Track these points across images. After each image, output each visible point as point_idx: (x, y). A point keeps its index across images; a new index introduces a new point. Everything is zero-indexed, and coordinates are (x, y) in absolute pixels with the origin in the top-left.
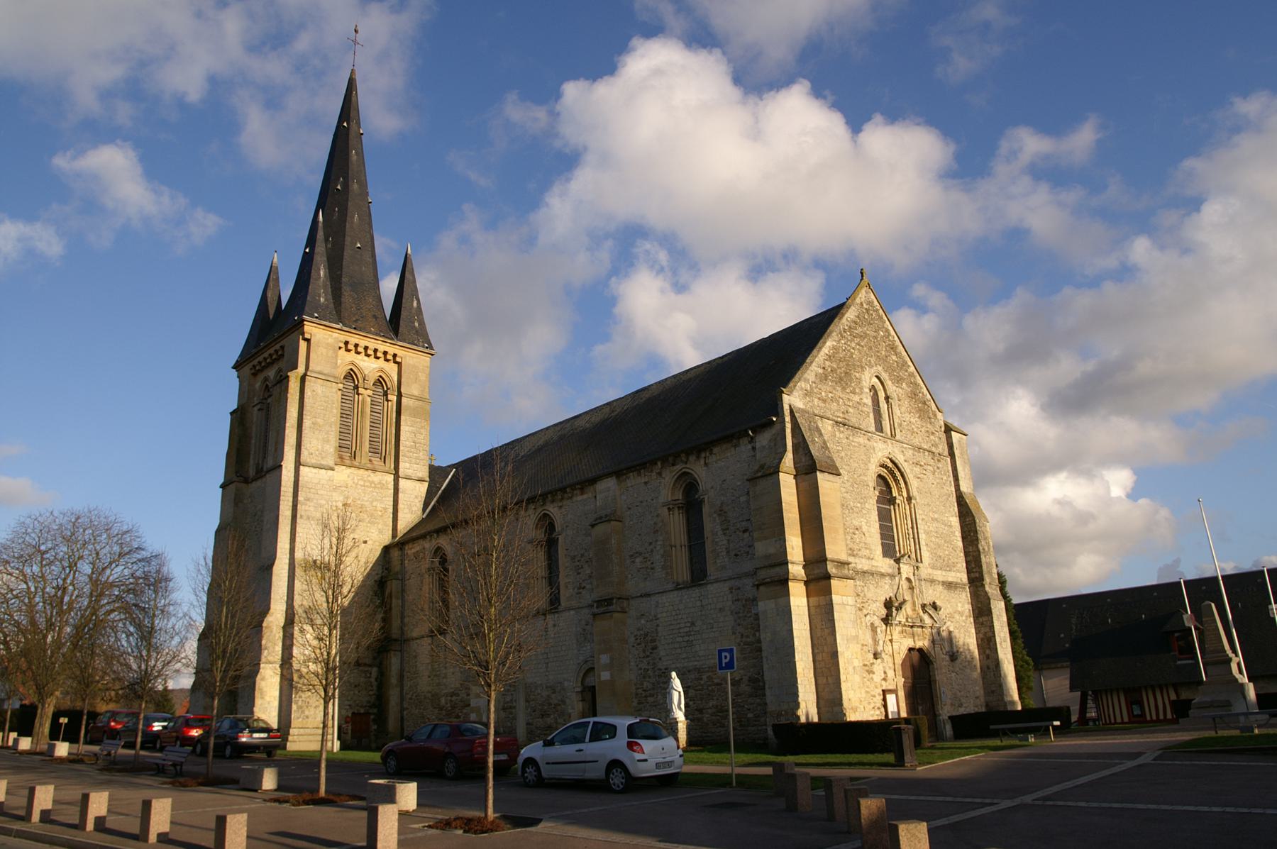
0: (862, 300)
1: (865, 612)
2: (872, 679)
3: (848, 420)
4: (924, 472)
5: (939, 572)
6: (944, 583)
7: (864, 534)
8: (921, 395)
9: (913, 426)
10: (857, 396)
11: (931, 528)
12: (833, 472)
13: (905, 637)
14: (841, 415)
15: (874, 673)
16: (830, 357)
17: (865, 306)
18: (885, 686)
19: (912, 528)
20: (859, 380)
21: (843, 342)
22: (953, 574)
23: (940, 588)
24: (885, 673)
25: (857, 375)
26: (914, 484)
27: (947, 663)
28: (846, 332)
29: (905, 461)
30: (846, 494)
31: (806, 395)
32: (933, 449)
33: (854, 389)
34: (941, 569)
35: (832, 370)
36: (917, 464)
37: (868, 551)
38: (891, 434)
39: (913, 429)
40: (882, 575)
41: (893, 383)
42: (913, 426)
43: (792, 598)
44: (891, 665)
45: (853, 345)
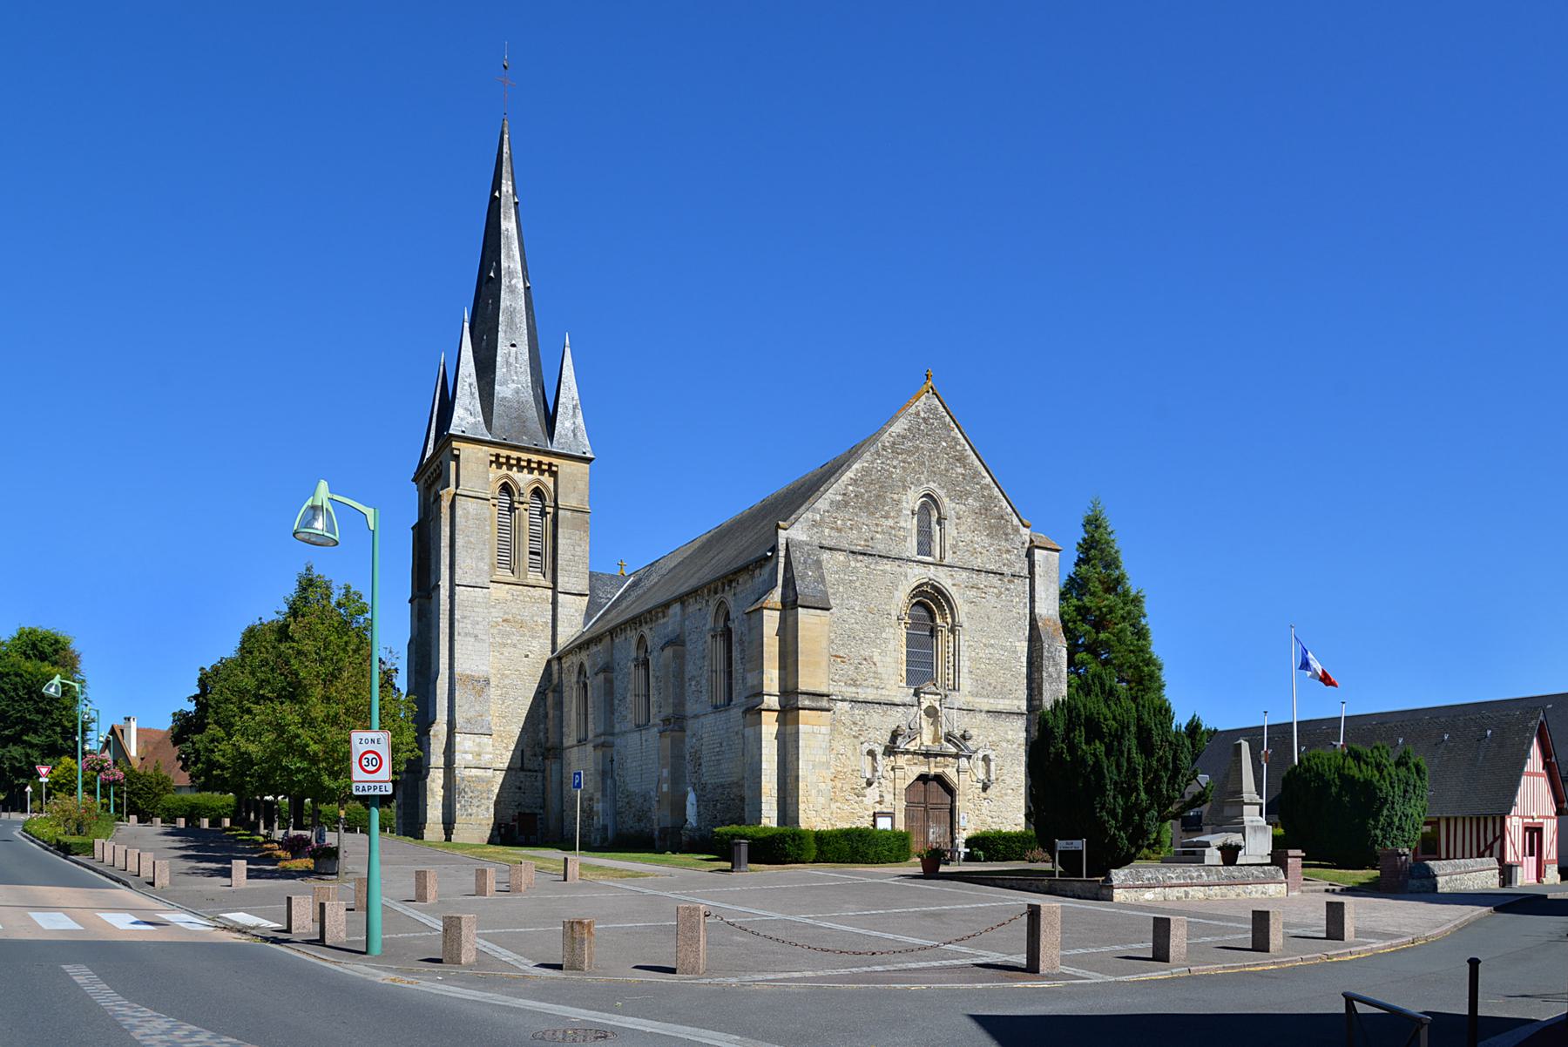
0: (919, 408)
1: (862, 739)
2: (862, 801)
4: (983, 595)
5: (986, 700)
7: (875, 665)
8: (997, 509)
9: (976, 546)
10: (890, 520)
11: (980, 655)
13: (916, 764)
14: (863, 543)
15: (865, 796)
16: (856, 481)
17: (922, 415)
19: (954, 655)
20: (898, 502)
21: (879, 461)
22: (1007, 702)
24: (881, 796)
25: (895, 497)
26: (962, 609)
28: (885, 450)
29: (954, 585)
30: (855, 625)
31: (813, 525)
32: (1005, 570)
33: (887, 512)
35: (856, 496)
36: (972, 587)
37: (877, 681)
38: (941, 558)
39: (975, 549)
41: (950, 500)
42: (976, 546)
43: (764, 727)
44: (892, 790)
45: (895, 463)
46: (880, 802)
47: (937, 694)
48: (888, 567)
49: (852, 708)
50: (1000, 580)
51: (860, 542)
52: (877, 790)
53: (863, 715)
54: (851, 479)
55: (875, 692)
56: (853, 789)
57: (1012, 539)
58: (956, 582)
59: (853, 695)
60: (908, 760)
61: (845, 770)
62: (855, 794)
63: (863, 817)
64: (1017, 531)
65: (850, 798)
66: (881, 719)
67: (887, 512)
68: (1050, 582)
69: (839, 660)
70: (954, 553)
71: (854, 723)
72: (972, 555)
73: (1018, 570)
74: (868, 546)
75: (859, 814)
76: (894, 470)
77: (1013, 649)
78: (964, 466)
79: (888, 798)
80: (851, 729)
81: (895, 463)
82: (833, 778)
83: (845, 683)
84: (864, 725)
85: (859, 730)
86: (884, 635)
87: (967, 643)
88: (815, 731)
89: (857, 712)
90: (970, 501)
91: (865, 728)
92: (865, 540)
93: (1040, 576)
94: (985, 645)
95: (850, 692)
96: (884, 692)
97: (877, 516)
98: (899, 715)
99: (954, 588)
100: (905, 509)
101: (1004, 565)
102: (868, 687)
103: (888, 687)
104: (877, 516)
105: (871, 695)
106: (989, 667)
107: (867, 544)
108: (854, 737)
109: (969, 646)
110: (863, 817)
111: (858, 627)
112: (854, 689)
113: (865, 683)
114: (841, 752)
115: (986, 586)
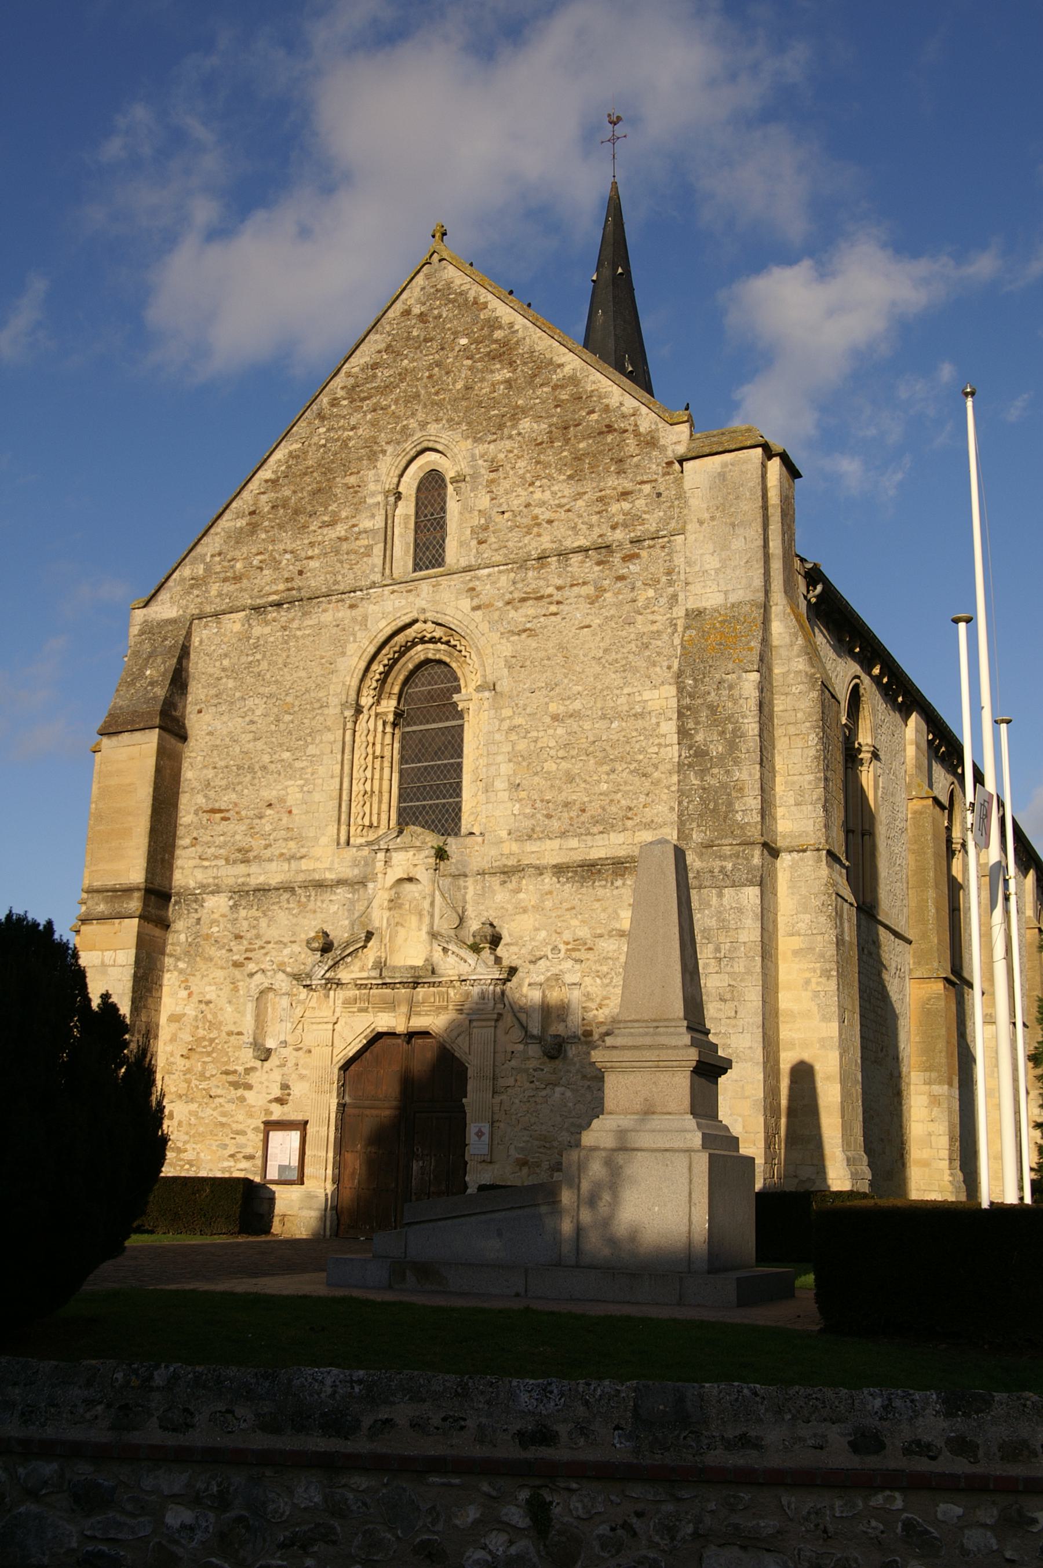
2: (242, 1099)
3: (299, 589)
4: (553, 608)
5: (556, 844)
6: (559, 870)
7: (290, 812)
9: (537, 511)
12: (137, 726)
15: (249, 1087)
18: (277, 1113)
20: (355, 489)
23: (548, 880)
24: (285, 1087)
25: (352, 480)
27: (532, 1064)
33: (334, 514)
34: (563, 834)
36: (523, 600)
37: (292, 844)
39: (536, 518)
40: (320, 885)
42: (537, 511)
46: (281, 1101)
47: (419, 849)
48: (327, 617)
49: (234, 907)
50: (599, 563)
51: (274, 588)
52: (277, 1076)
53: (256, 919)
54: (266, 481)
55: (286, 866)
56: (227, 1073)
57: (637, 466)
58: (484, 599)
59: (240, 880)
60: (347, 1002)
61: (211, 1036)
62: (231, 1084)
63: (243, 1133)
64: (650, 442)
65: (219, 1092)
66: (294, 921)
67: (334, 514)
68: (733, 525)
69: (218, 816)
70: (480, 543)
71: (238, 937)
72: (529, 533)
73: (653, 529)
74: (292, 589)
75: (235, 1126)
76: (351, 433)
77: (638, 709)
78: (511, 363)
79: (298, 1089)
80: (231, 950)
81: (357, 417)
82: (185, 1052)
83: (227, 860)
84: (258, 936)
85: (247, 950)
86: (311, 750)
87: (506, 725)
88: (107, 962)
89: (243, 913)
90: (526, 424)
91: (260, 943)
92: (287, 580)
93: (701, 523)
94: (555, 718)
95: (233, 874)
96: (304, 864)
97: (312, 528)
98: (334, 908)
99: (479, 613)
100: (373, 494)
101: (614, 528)
102: (270, 860)
103: (317, 851)
104: (312, 528)
105: (273, 874)
106: (564, 765)
107: (289, 585)
108: (237, 965)
109: (512, 729)
110: (243, 1133)
111: (260, 744)
112: (242, 869)
113: (268, 853)
114: (208, 997)
115: (559, 588)
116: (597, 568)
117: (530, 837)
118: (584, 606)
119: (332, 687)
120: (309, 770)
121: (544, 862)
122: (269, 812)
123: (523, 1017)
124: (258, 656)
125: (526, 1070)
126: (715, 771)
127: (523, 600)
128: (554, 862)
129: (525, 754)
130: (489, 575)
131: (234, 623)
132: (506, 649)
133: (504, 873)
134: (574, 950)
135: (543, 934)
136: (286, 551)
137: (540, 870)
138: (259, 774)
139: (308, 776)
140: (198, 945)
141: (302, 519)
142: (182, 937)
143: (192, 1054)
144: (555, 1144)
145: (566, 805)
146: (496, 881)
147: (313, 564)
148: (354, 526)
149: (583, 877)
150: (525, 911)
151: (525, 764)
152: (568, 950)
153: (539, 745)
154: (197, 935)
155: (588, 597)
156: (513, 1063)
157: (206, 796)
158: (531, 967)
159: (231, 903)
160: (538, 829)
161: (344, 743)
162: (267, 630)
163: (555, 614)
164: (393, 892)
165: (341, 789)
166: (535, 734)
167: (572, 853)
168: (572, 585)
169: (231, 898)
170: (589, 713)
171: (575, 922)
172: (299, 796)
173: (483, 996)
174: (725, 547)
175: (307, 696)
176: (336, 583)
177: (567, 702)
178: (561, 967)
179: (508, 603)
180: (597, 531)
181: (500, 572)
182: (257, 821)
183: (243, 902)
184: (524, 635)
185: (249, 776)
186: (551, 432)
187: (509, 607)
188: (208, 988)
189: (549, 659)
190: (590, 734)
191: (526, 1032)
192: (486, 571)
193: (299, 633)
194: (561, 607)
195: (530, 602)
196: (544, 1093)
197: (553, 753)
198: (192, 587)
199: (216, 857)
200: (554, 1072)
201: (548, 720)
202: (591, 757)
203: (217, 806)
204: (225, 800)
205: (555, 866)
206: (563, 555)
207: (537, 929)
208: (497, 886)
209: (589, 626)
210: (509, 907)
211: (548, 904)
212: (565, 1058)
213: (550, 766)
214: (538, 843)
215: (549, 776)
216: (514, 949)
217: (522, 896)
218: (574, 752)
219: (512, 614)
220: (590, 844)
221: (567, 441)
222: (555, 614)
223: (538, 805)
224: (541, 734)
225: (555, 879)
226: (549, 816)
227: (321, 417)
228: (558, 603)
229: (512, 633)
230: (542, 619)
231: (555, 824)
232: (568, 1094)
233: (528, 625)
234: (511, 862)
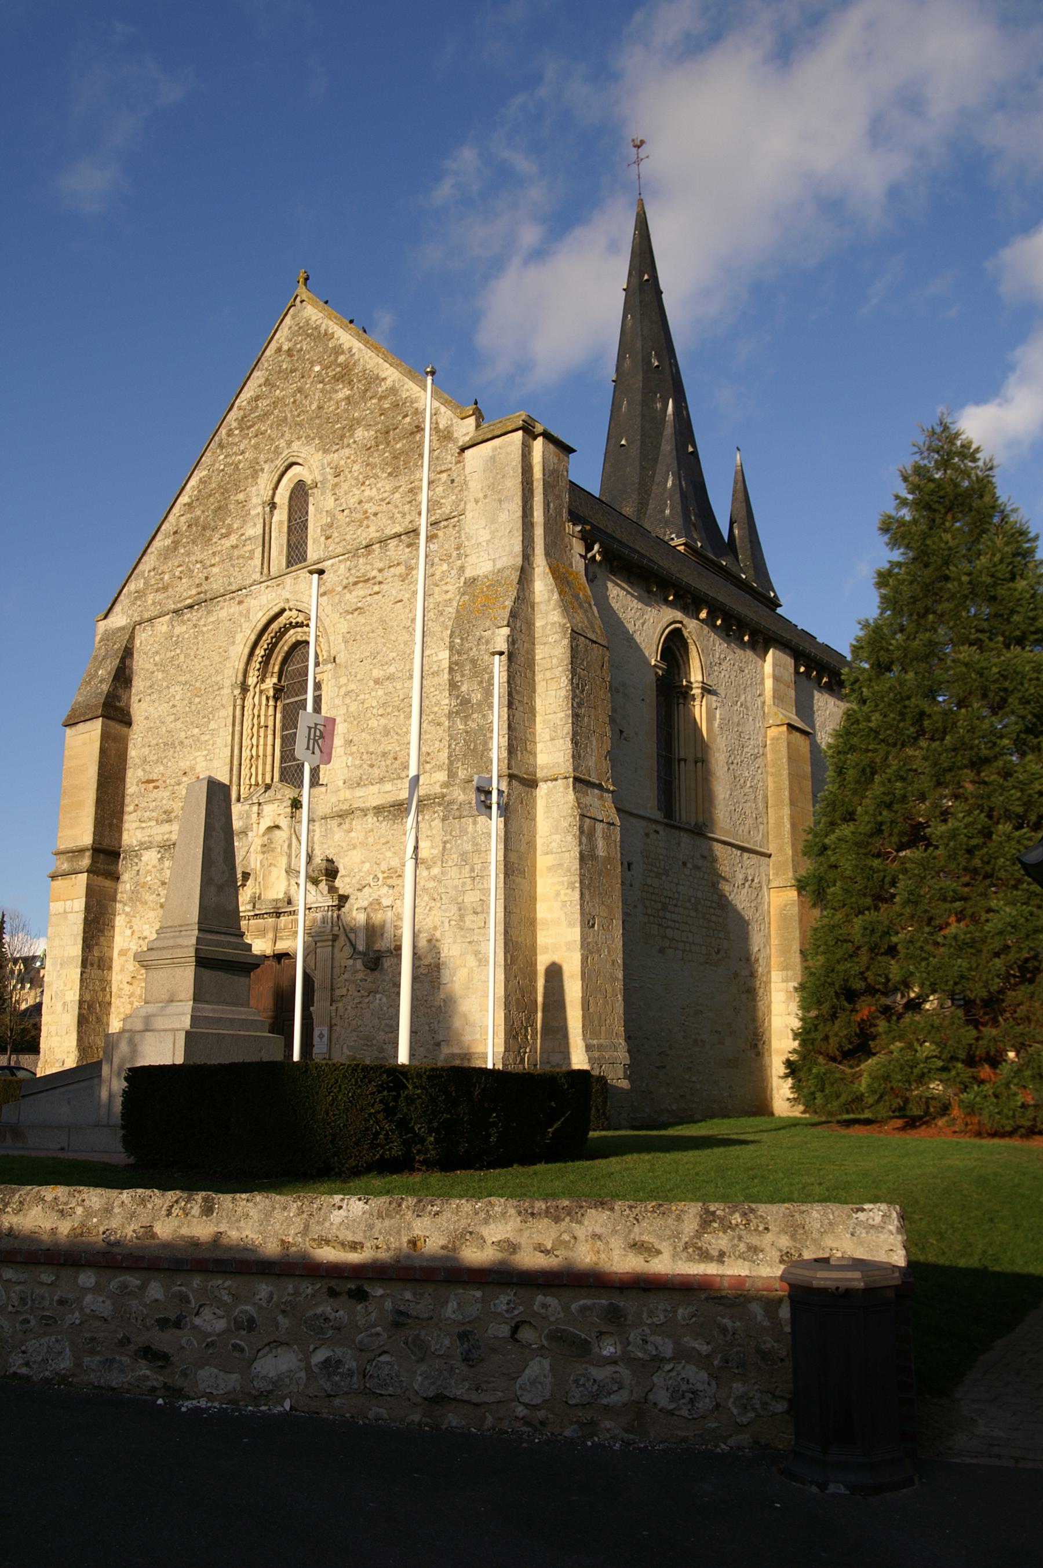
3: (206, 592)
4: (376, 588)
5: (375, 789)
6: (378, 810)
9: (367, 506)
12: (87, 717)
20: (242, 504)
23: (371, 819)
25: (241, 497)
27: (360, 976)
34: (381, 780)
36: (356, 583)
42: (367, 506)
48: (223, 614)
49: (161, 859)
50: (408, 546)
51: (190, 593)
54: (185, 505)
68: (500, 501)
70: (327, 538)
73: (448, 512)
76: (241, 457)
83: (157, 821)
86: (213, 725)
88: (68, 910)
90: (360, 433)
93: (477, 501)
94: (377, 682)
97: (214, 540)
99: (325, 598)
100: (255, 507)
106: (383, 721)
107: (199, 589)
111: (179, 724)
114: (145, 934)
115: (380, 571)
116: (407, 550)
117: (359, 784)
118: (398, 583)
119: (226, 671)
120: (211, 742)
121: (368, 805)
122: (185, 779)
123: (352, 936)
124: (178, 651)
125: (355, 981)
126: (475, 716)
127: (356, 583)
128: (375, 804)
129: (355, 714)
130: (332, 565)
131: (162, 626)
132: (343, 627)
133: (340, 816)
134: (388, 877)
135: (367, 865)
136: (197, 562)
137: (365, 812)
138: (178, 749)
139: (210, 747)
140: (138, 892)
141: (208, 533)
142: (128, 886)
143: (134, 981)
144: (374, 1042)
145: (384, 754)
146: (334, 823)
147: (215, 570)
148: (242, 535)
149: (394, 815)
150: (354, 848)
151: (355, 723)
152: (384, 878)
153: (366, 706)
154: (137, 884)
155: (400, 575)
156: (346, 976)
157: (143, 770)
158: (359, 894)
159: (159, 856)
160: (364, 777)
161: (234, 717)
162: (184, 628)
163: (377, 593)
164: (266, 838)
165: (232, 756)
166: (362, 697)
167: (387, 795)
168: (390, 567)
169: (159, 852)
170: (400, 675)
171: (389, 854)
172: (204, 764)
173: (324, 920)
174: (493, 521)
175: (209, 681)
176: (230, 584)
177: (385, 667)
178: (379, 893)
179: (345, 587)
180: (408, 518)
181: (340, 562)
182: (176, 787)
183: (167, 855)
184: (356, 613)
185: (172, 751)
186: (376, 437)
187: (346, 591)
188: (145, 927)
189: (373, 632)
190: (401, 693)
191: (355, 949)
192: (330, 562)
193: (205, 629)
194: (382, 586)
195: (361, 585)
196: (367, 1000)
197: (375, 711)
198: (136, 598)
199: (150, 820)
200: (374, 982)
201: (371, 683)
202: (401, 713)
203: (150, 777)
204: (157, 771)
205: (375, 808)
206: (383, 541)
207: (363, 862)
208: (336, 829)
209: (401, 601)
210: (344, 844)
211: (371, 840)
212: (382, 968)
213: (373, 723)
214: (364, 789)
215: (372, 732)
216: (347, 880)
217: (353, 834)
218: (389, 710)
219: (348, 596)
220: (400, 786)
221: (388, 444)
222: (377, 593)
223: (365, 757)
224: (367, 696)
225: (375, 819)
226: (372, 766)
227: (221, 446)
228: (380, 583)
229: (348, 612)
230: (368, 598)
231: (376, 772)
232: (384, 999)
233: (359, 605)
234: (345, 807)
